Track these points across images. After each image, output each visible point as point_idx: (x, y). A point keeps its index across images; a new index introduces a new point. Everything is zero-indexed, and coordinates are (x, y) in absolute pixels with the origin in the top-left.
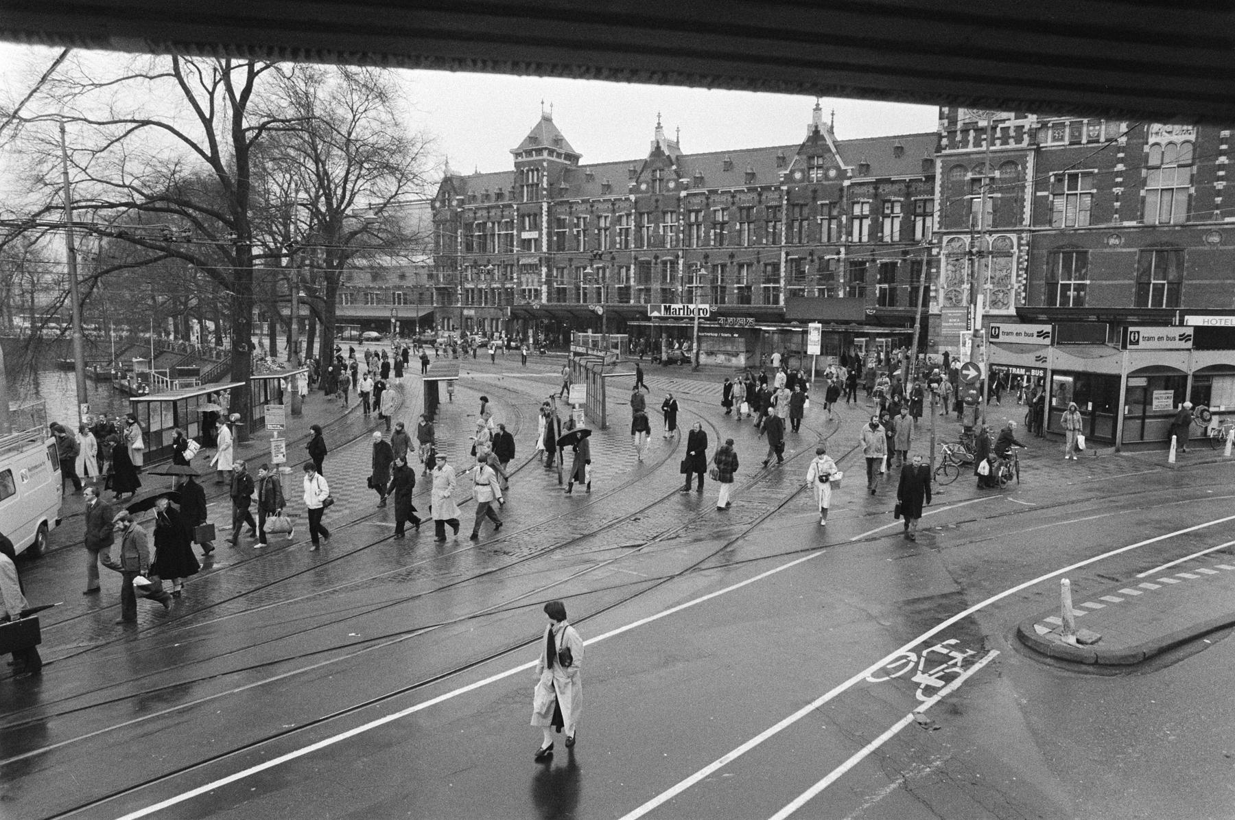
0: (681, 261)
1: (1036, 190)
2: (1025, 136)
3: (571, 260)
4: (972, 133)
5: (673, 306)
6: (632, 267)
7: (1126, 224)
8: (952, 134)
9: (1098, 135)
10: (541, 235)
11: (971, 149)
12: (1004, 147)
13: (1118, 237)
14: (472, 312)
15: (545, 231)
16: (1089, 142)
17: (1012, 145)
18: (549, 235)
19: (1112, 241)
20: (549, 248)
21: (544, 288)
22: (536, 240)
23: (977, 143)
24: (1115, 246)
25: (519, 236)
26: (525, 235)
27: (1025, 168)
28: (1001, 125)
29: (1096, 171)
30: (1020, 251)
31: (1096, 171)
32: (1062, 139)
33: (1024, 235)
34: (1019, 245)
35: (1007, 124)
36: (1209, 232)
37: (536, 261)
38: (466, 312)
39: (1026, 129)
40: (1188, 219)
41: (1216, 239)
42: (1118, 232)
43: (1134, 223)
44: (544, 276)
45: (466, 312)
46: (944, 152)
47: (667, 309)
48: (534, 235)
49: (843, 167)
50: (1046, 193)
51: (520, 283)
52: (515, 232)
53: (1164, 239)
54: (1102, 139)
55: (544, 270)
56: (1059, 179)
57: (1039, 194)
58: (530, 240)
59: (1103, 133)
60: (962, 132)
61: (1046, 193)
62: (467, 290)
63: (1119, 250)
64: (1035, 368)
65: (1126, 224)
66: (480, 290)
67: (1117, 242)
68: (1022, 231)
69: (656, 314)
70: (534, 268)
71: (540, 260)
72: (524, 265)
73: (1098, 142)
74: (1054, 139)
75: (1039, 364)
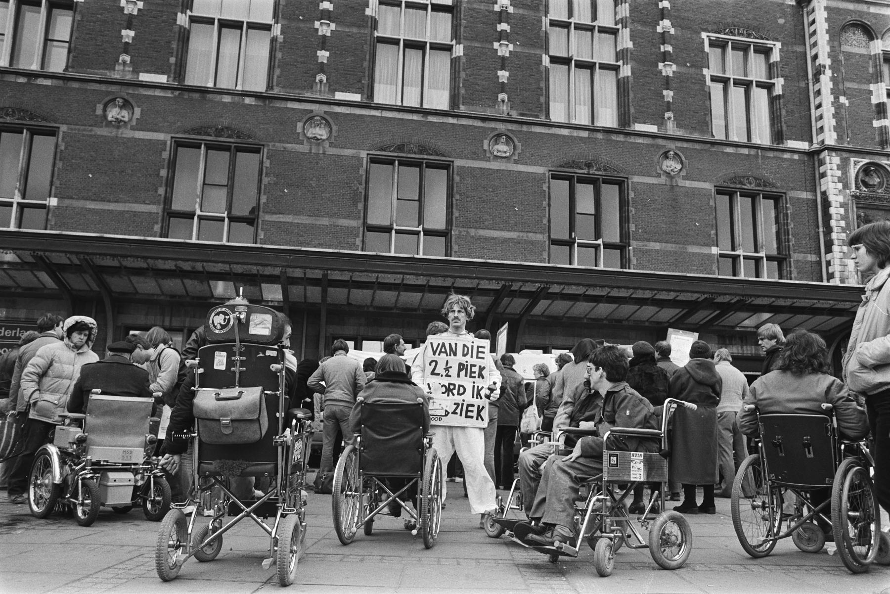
7: (144, 77)
13: (126, 105)
19: (113, 113)
24: (119, 123)
36: (310, 118)
40: (270, 86)
41: (321, 132)
42: (128, 92)
43: (162, 79)
53: (225, 121)
63: (128, 133)
67: (125, 115)
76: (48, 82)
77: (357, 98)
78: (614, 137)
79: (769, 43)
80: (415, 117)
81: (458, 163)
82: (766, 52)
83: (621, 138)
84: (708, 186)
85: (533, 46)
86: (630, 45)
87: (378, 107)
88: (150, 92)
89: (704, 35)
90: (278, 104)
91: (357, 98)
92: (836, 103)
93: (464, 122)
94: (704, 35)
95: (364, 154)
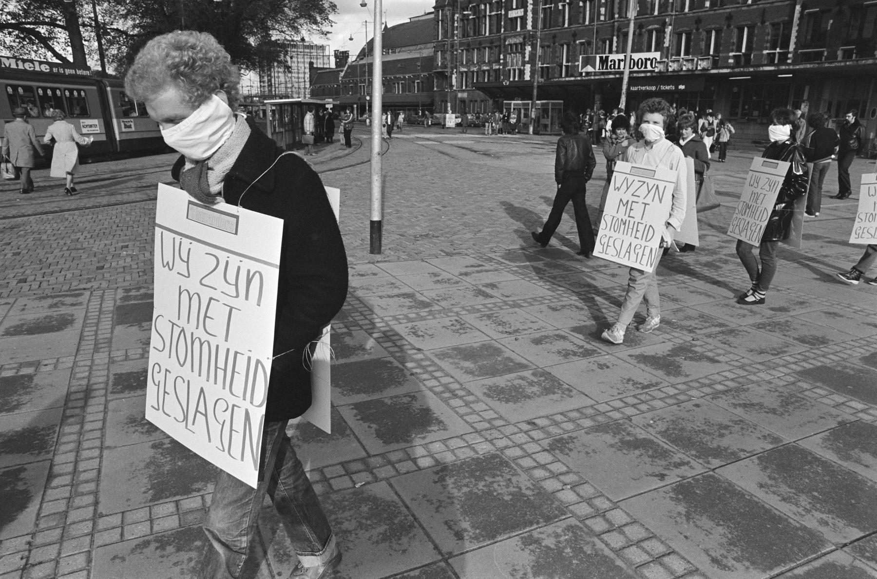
0: (669, 29)
3: (554, 37)
5: (612, 57)
6: (615, 39)
10: (526, 12)
14: (465, 95)
15: (530, 7)
18: (535, 12)
20: (534, 26)
21: (528, 68)
22: (521, 18)
25: (506, 14)
26: (512, 14)
37: (519, 40)
38: (460, 95)
44: (527, 55)
45: (460, 95)
47: (604, 61)
48: (520, 13)
51: (505, 64)
52: (503, 12)
55: (528, 49)
58: (516, 18)
62: (462, 73)
66: (473, 72)
69: (589, 69)
70: (519, 49)
71: (524, 38)
72: (511, 45)
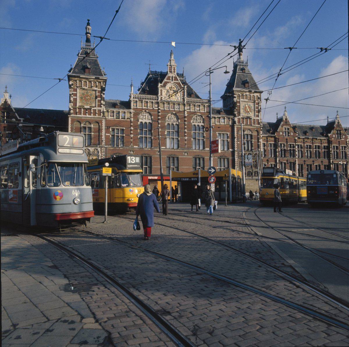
1: (106, 133)
2: (102, 113)
4: (82, 110)
7: (135, 147)
8: (75, 109)
9: (125, 117)
11: (82, 115)
12: (99, 116)
16: (122, 118)
17: (97, 116)
23: (85, 114)
27: (102, 125)
28: (93, 108)
29: (125, 128)
30: (102, 154)
31: (125, 128)
32: (113, 116)
33: (103, 149)
34: (101, 152)
35: (95, 108)
39: (102, 111)
43: (137, 147)
46: (71, 115)
49: (19, 118)
50: (109, 134)
53: (146, 153)
54: (126, 118)
56: (113, 130)
57: (107, 134)
59: (126, 116)
60: (78, 108)
61: (109, 134)
64: (193, 178)
65: (135, 147)
68: (102, 147)
73: (125, 119)
74: (111, 116)
75: (195, 176)
76: (121, 148)
77: (164, 148)
78: (202, 151)
79: (228, 133)
80: (173, 150)
81: (180, 157)
82: (227, 134)
83: (203, 151)
84: (217, 158)
85: (190, 137)
86: (205, 135)
87: (168, 149)
88: (135, 149)
89: (217, 133)
90: (153, 149)
91: (164, 148)
92: (237, 143)
93: (180, 150)
94: (217, 133)
95: (166, 156)
